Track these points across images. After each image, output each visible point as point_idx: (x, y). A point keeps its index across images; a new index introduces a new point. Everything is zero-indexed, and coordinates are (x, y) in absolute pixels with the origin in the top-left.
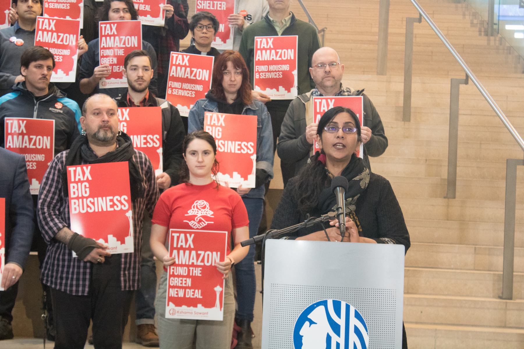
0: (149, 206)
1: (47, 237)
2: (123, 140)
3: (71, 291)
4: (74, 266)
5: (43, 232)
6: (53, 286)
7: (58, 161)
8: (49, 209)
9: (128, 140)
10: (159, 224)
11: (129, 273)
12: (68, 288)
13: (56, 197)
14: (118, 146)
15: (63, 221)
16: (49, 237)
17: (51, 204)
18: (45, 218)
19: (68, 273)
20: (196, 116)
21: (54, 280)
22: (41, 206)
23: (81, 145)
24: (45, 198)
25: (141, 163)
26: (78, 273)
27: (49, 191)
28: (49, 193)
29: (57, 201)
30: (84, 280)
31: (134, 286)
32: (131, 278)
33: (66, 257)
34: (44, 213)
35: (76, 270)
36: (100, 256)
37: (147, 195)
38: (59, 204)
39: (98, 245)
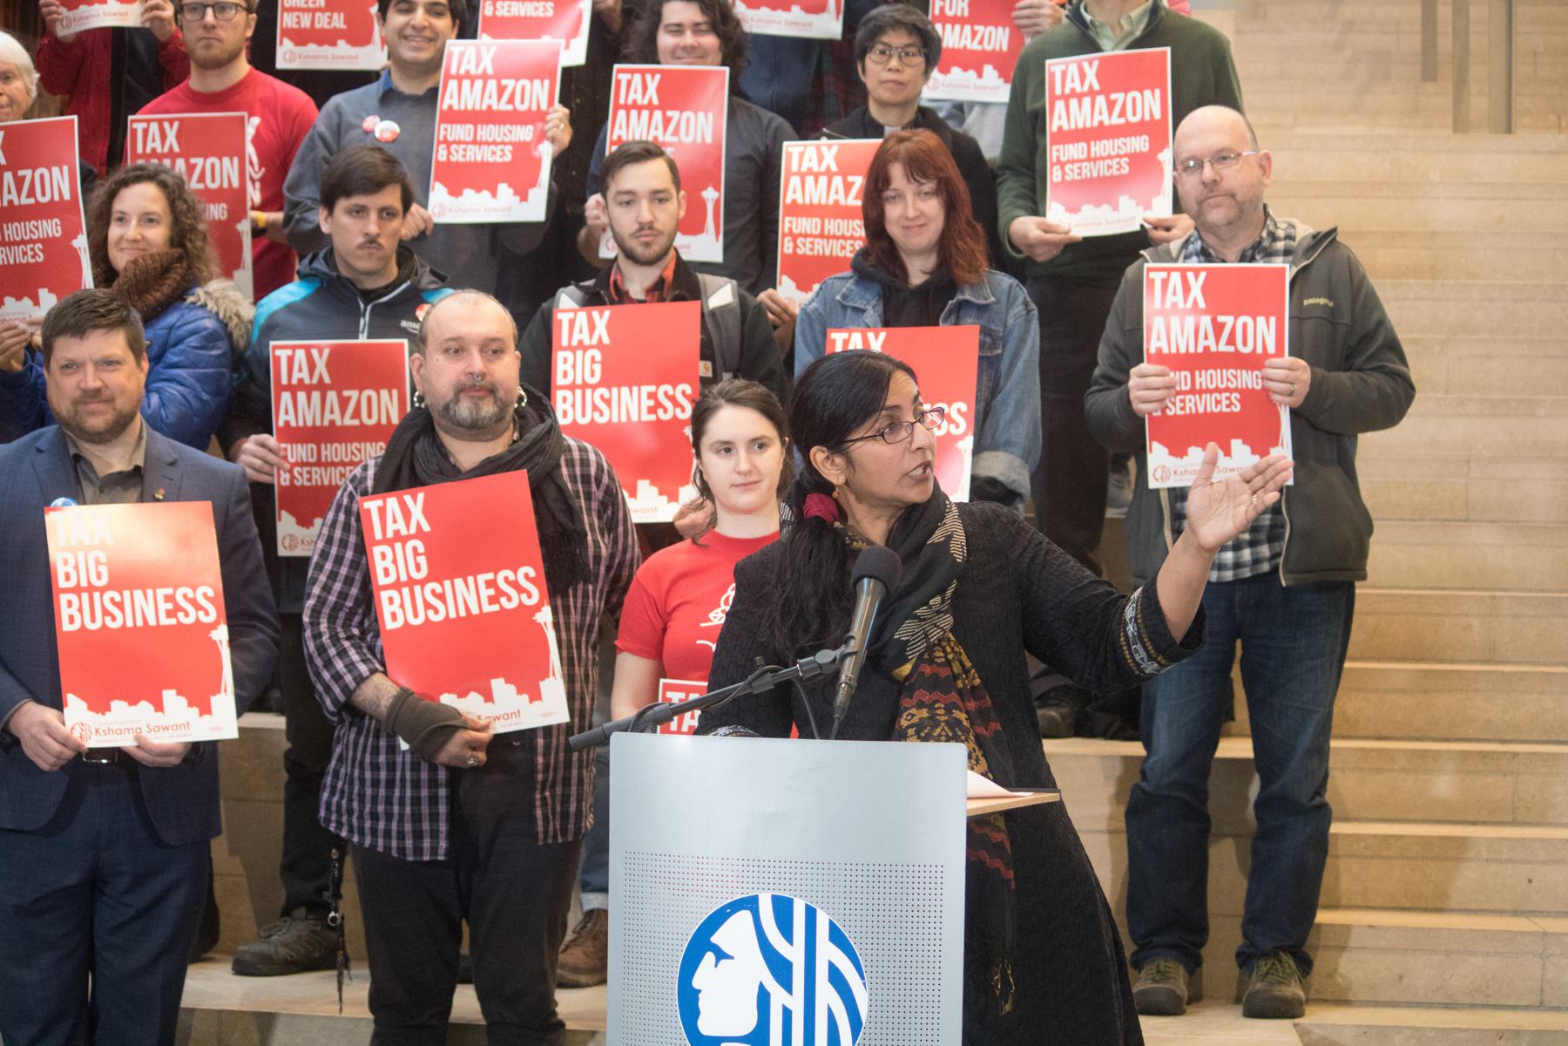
0: (614, 600)
1: (328, 702)
2: (535, 414)
3: (402, 850)
4: (403, 780)
5: (319, 687)
6: (356, 839)
7: (355, 488)
8: (334, 623)
9: (546, 417)
10: (631, 651)
11: (553, 796)
12: (394, 844)
13: (354, 591)
14: (516, 436)
15: (374, 655)
16: (335, 701)
17: (341, 609)
18: (322, 650)
19: (389, 801)
20: (817, 326)
21: (355, 822)
22: (311, 617)
23: (415, 439)
24: (324, 595)
25: (586, 479)
26: (416, 801)
27: (333, 576)
28: (335, 581)
29: (357, 600)
30: (434, 818)
31: (564, 834)
32: (558, 808)
33: (382, 758)
34: (317, 636)
35: (408, 793)
36: (474, 749)
37: (608, 569)
38: (360, 611)
39: (465, 721)
